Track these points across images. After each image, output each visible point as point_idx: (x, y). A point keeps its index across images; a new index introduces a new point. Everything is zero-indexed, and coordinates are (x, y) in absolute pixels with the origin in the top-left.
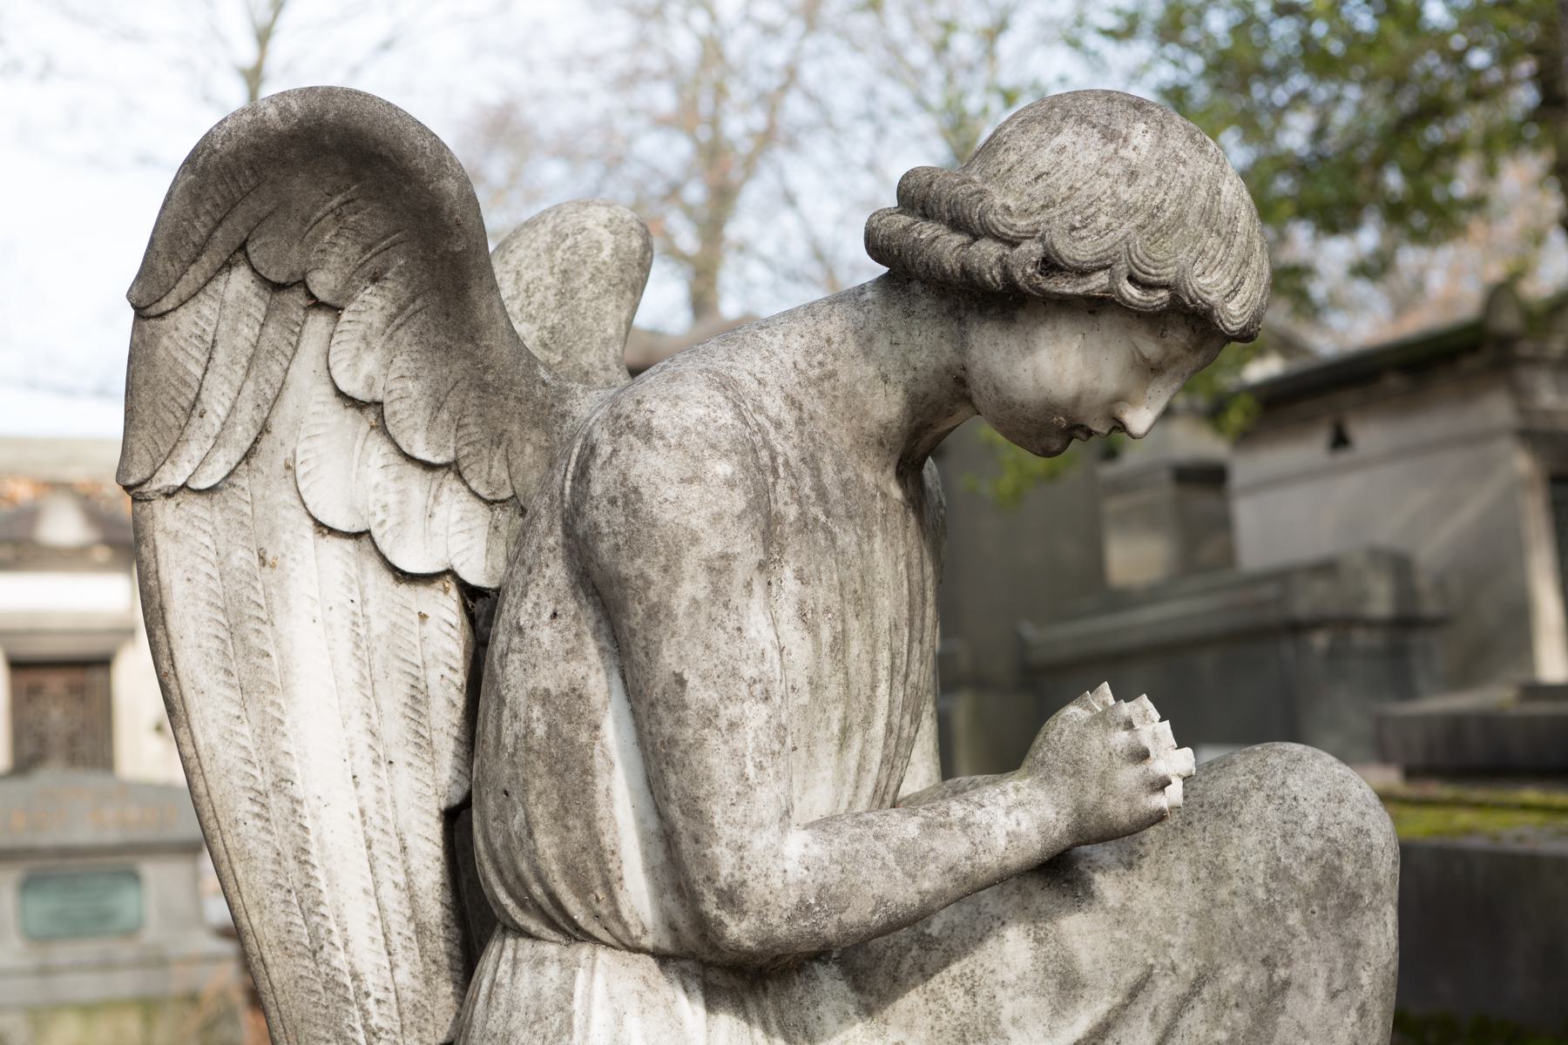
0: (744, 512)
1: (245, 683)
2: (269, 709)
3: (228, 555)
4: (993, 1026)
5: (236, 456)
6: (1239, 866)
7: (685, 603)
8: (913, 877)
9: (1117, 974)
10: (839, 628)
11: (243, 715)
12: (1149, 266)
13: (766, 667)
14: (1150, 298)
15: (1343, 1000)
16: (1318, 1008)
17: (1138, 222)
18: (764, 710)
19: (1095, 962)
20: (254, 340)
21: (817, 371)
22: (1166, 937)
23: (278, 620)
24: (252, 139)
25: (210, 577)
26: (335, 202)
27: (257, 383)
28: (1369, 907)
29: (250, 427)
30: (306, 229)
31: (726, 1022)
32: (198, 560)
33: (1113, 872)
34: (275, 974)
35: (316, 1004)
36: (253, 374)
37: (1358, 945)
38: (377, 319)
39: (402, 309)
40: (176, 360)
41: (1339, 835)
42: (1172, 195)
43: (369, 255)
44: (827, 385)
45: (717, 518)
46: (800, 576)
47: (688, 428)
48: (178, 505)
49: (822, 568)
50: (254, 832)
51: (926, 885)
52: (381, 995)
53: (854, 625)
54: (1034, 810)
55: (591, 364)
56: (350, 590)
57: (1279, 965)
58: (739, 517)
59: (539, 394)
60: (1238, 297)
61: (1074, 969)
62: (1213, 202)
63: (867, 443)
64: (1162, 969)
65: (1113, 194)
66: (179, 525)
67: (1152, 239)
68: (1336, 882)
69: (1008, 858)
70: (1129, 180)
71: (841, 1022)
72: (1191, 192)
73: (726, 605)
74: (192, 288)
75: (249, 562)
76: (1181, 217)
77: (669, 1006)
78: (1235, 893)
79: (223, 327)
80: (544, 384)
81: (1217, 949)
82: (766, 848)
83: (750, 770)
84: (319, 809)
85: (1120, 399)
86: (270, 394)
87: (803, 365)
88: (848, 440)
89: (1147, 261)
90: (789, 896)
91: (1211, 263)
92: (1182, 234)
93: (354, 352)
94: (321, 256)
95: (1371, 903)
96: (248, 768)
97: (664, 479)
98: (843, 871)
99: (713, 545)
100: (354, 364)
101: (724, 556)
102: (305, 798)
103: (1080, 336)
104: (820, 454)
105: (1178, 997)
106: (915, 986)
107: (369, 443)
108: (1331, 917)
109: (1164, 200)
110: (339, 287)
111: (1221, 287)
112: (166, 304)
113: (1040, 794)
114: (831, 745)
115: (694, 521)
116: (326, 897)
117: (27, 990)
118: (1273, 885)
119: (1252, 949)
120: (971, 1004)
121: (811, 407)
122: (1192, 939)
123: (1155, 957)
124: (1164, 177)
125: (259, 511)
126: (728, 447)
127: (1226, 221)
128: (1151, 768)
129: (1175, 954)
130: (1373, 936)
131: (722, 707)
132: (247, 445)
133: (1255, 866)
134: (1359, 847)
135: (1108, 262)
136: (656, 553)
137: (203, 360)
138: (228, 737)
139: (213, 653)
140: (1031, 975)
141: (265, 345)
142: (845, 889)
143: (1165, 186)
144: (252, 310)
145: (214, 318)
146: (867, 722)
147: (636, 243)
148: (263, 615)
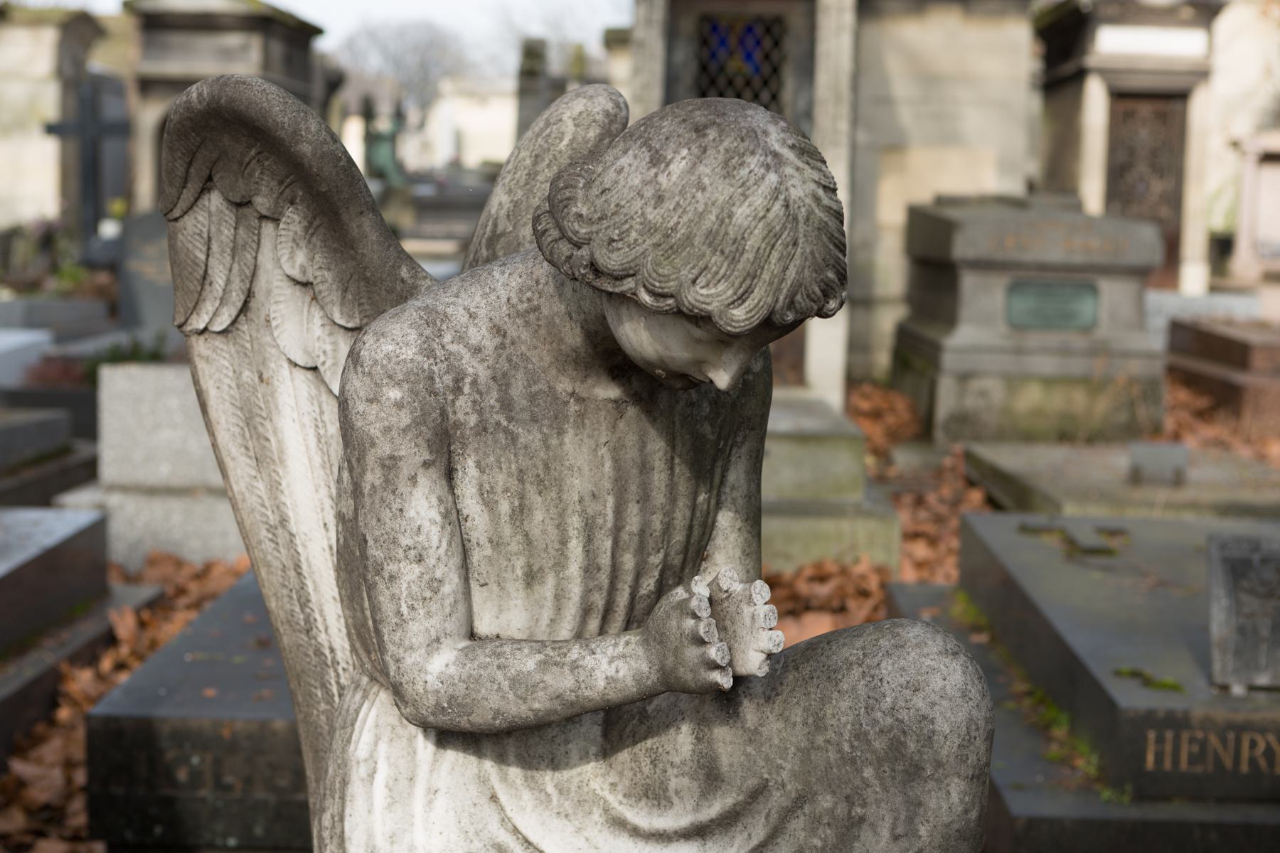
0: (409, 426)
1: (258, 456)
2: (273, 474)
3: (241, 373)
4: (664, 791)
5: (234, 312)
6: (834, 722)
7: (368, 487)
8: (525, 700)
9: (744, 779)
10: (517, 503)
11: (259, 476)
12: (654, 280)
13: (422, 538)
14: (659, 304)
16: (883, 844)
17: (654, 241)
18: (417, 569)
19: (731, 765)
20: (232, 238)
21: (525, 305)
22: (779, 762)
23: (275, 417)
24: (186, 114)
25: (230, 387)
26: (253, 152)
27: (240, 265)
28: (931, 777)
29: (240, 293)
30: (243, 168)
32: (222, 376)
33: (756, 701)
34: (286, 640)
35: (309, 663)
36: (236, 259)
37: (920, 804)
39: (311, 223)
40: (188, 249)
41: (906, 718)
42: (685, 219)
43: (283, 188)
44: (532, 317)
45: (387, 430)
46: (478, 465)
47: (377, 360)
48: (206, 340)
49: (503, 460)
50: (270, 550)
51: (536, 706)
52: (345, 666)
53: (535, 499)
54: (633, 663)
55: (524, 237)
56: (312, 404)
57: (856, 804)
58: (404, 430)
59: (399, 288)
60: (747, 304)
61: (716, 767)
62: (721, 226)
63: (566, 361)
64: (775, 783)
65: (643, 214)
66: (208, 353)
67: (666, 255)
68: (902, 754)
69: (608, 694)
70: (656, 203)
71: (581, 759)
72: (701, 216)
73: (394, 492)
74: (188, 204)
75: (252, 380)
76: (689, 238)
77: (411, 739)
78: (829, 742)
79: (213, 229)
80: (403, 281)
81: (814, 780)
82: (414, 664)
83: (404, 609)
84: (306, 541)
85: (700, 363)
86: (248, 273)
87: (514, 300)
88: (548, 359)
89: (654, 275)
90: (429, 699)
91: (713, 277)
92: (689, 252)
93: (290, 250)
94: (256, 186)
95: (932, 775)
96: (263, 510)
97: (358, 396)
98: (467, 689)
99: (384, 449)
101: (392, 458)
102: (297, 533)
103: (643, 318)
104: (513, 372)
105: (783, 808)
106: (628, 747)
107: (313, 309)
108: (899, 778)
109: (679, 223)
110: (272, 207)
111: (724, 297)
112: (177, 213)
113: (640, 651)
114: (517, 583)
115: (372, 431)
116: (313, 598)
118: (856, 743)
119: (839, 787)
120: (653, 771)
121: (515, 334)
122: (796, 768)
123: (769, 773)
124: (681, 202)
125: (256, 346)
126: (401, 378)
127: (731, 242)
128: (707, 651)
129: (785, 775)
130: (934, 800)
131: (385, 564)
132: (239, 305)
133: (845, 725)
134: (921, 731)
135: (631, 272)
136: (355, 449)
137: (204, 249)
139: (237, 434)
140: (689, 763)
141: (240, 242)
142: (468, 700)
143: (680, 211)
144: (227, 218)
145: (206, 223)
146: (560, 564)
148: (264, 414)
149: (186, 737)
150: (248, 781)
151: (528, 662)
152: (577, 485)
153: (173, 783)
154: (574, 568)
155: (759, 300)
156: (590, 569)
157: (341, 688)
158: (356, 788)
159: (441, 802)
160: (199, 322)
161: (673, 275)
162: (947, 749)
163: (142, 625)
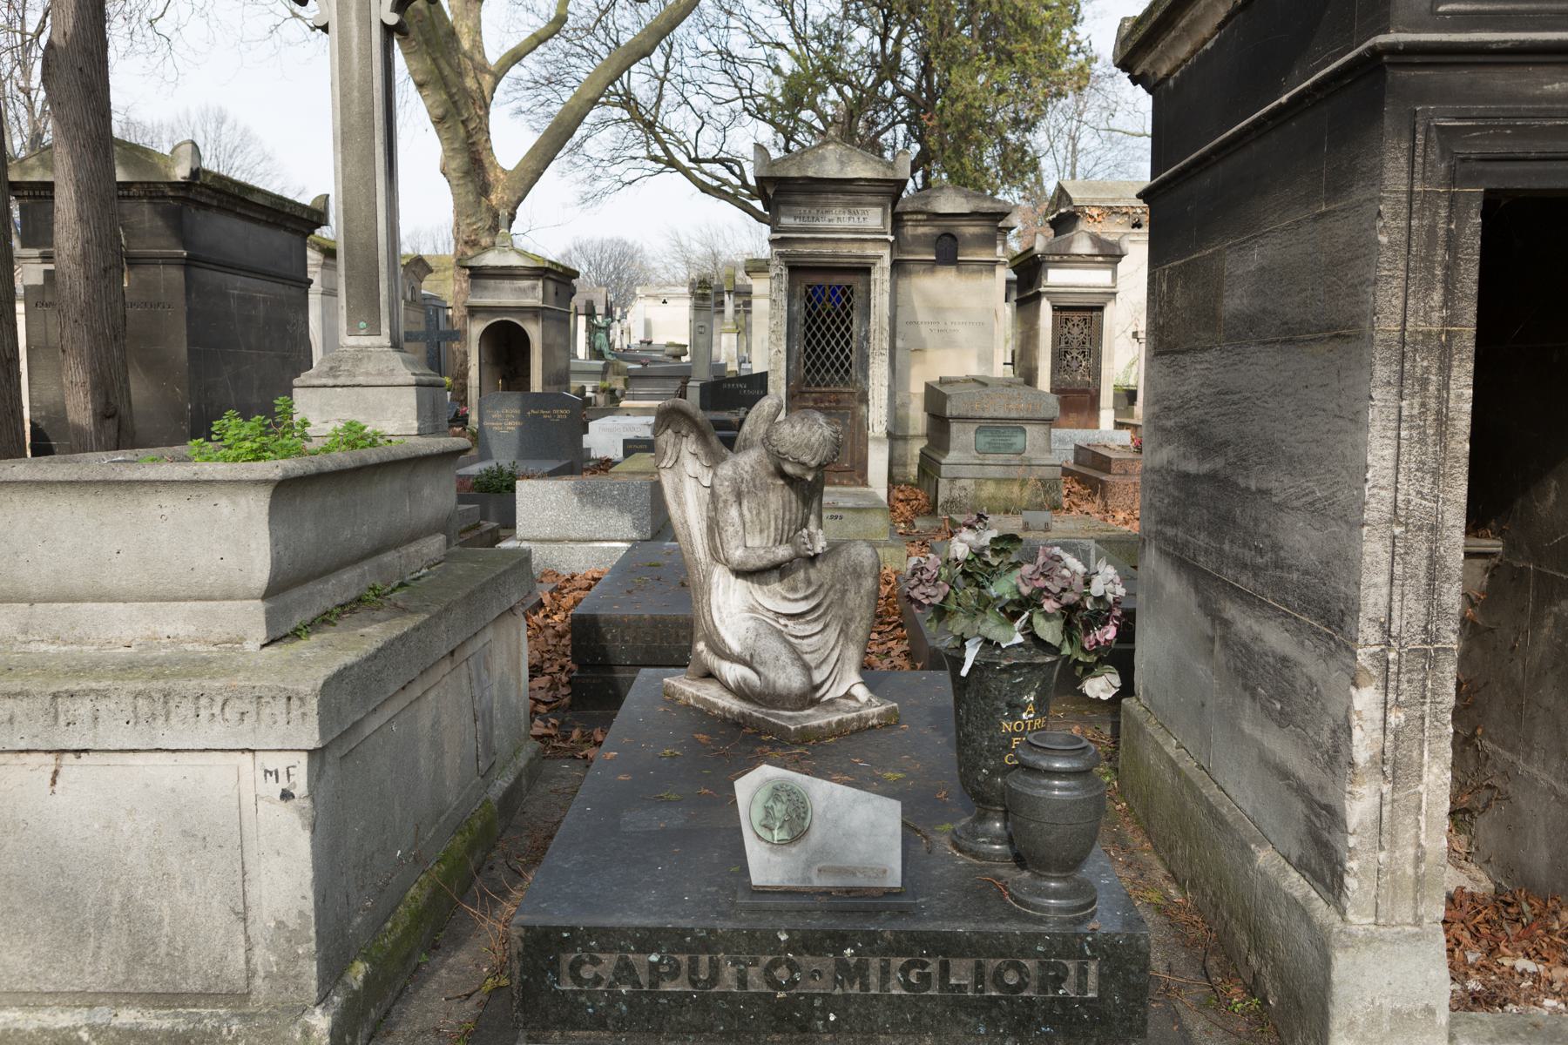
31: (739, 580)
117: (975, 471)
146: (769, 528)
149: (611, 622)
151: (762, 552)
152: (773, 507)
153: (606, 640)
154: (772, 529)
155: (818, 459)
156: (776, 529)
158: (713, 590)
160: (663, 465)
161: (798, 453)
162: (867, 570)
163: (554, 598)
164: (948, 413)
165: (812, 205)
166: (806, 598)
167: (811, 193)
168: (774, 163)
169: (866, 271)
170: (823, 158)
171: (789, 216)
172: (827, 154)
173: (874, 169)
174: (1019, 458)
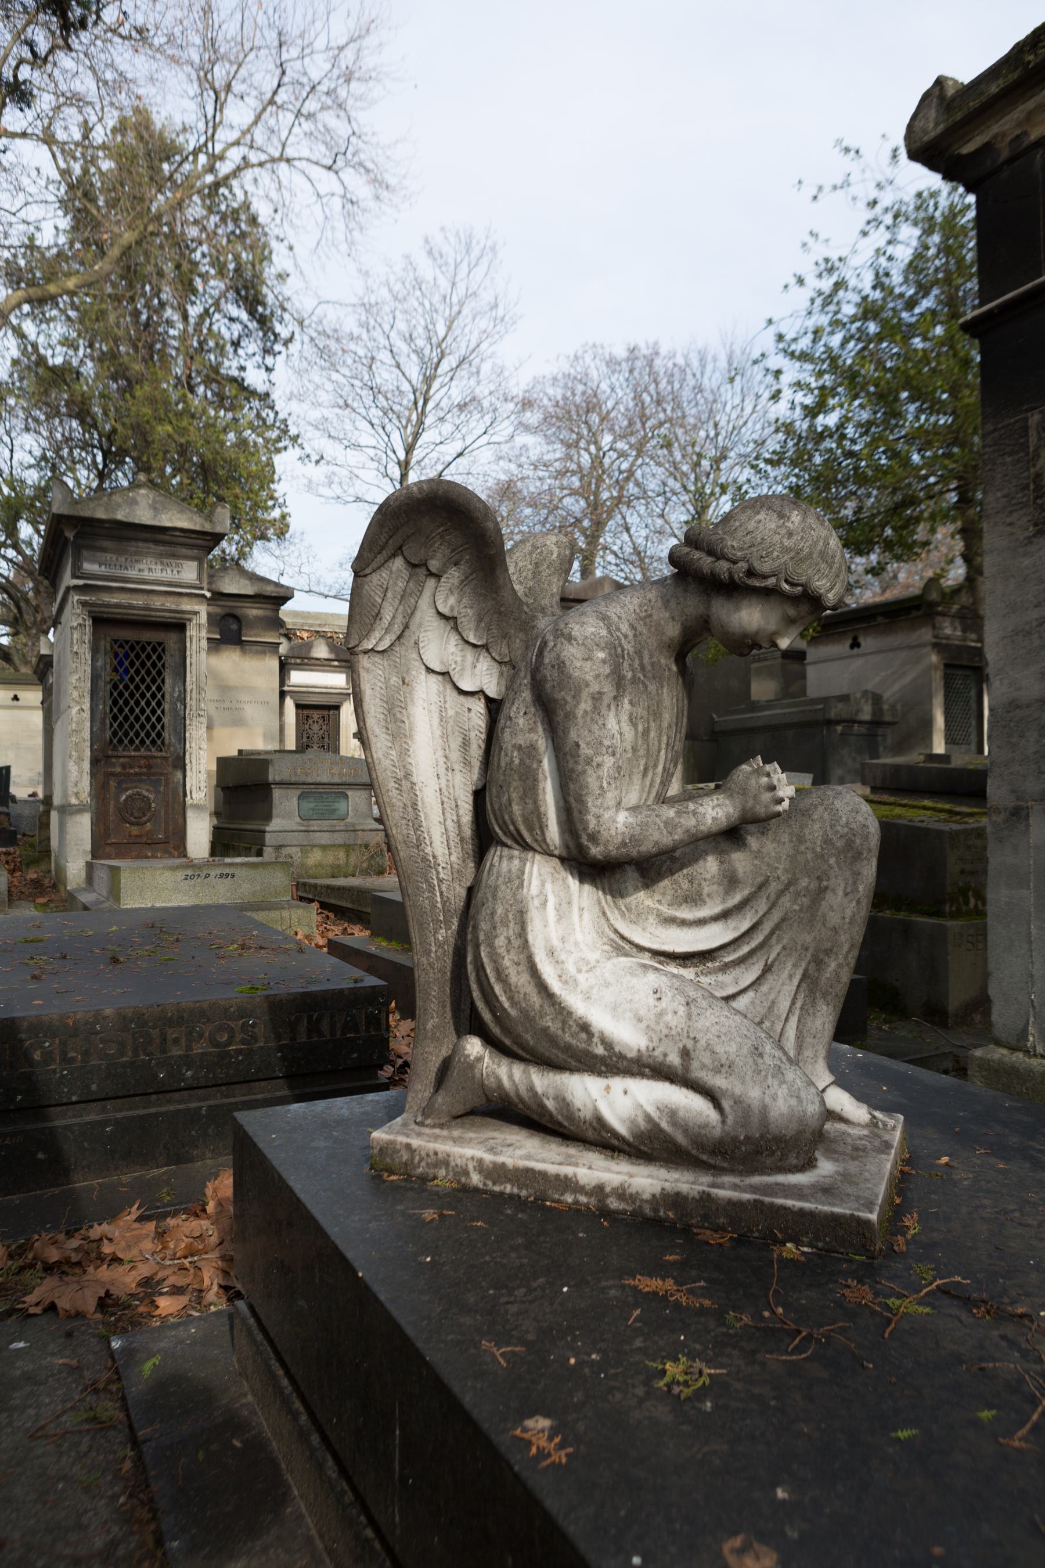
5: (394, 637)
15: (851, 897)
18: (612, 760)
31: (587, 888)
34: (401, 854)
38: (456, 582)
45: (597, 676)
46: (631, 702)
53: (653, 724)
72: (816, 543)
76: (810, 554)
77: (564, 880)
83: (605, 784)
85: (776, 634)
99: (595, 687)
100: (445, 601)
101: (600, 693)
112: (368, 571)
113: (727, 802)
116: (424, 824)
117: (300, 838)
138: (386, 755)
146: (655, 766)
147: (568, 552)
149: (41, 1028)
150: (86, 1054)
157: (440, 881)
159: (586, 915)
160: (368, 645)
164: (271, 779)
165: (120, 552)
166: (724, 916)
167: (120, 539)
168: (76, 502)
169: (179, 627)
170: (134, 502)
171: (92, 561)
172: (139, 499)
173: (191, 520)
174: (342, 823)
